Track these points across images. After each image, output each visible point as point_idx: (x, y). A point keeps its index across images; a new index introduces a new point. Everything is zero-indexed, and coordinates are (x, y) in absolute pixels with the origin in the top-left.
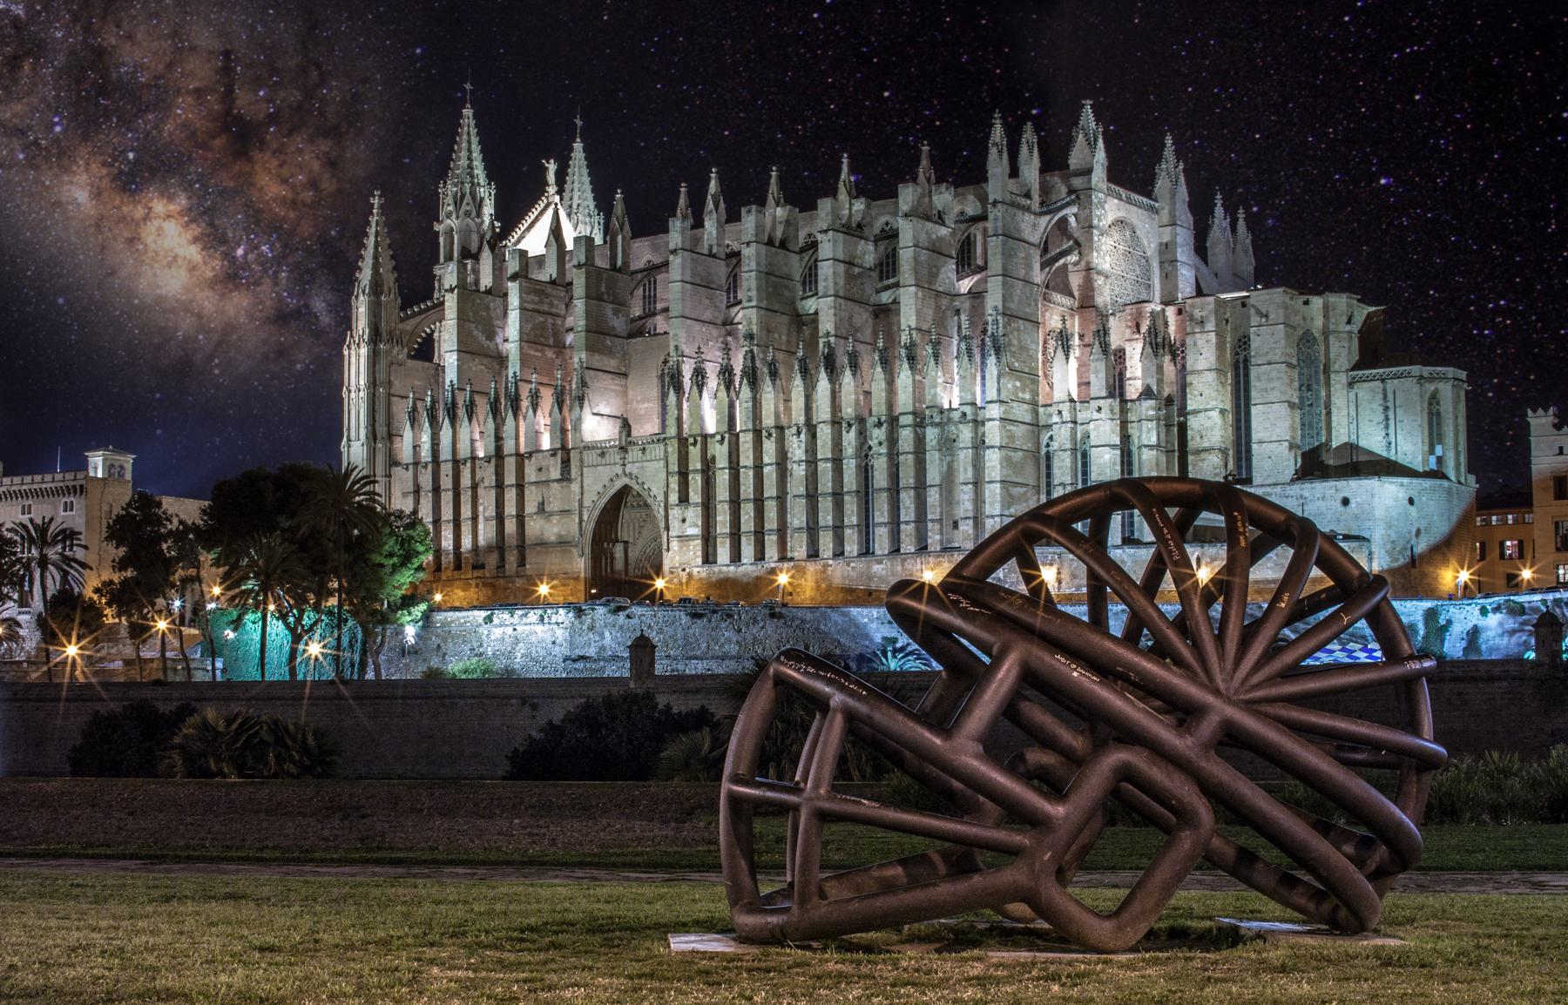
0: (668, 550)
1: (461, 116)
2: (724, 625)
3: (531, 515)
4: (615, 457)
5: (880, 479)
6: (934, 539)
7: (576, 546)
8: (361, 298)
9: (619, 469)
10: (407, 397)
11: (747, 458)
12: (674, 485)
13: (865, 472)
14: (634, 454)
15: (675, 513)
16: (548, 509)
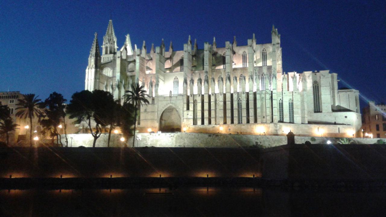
0: (183, 121)
1: (109, 21)
2: (216, 138)
3: (142, 112)
4: (169, 99)
5: (244, 105)
6: (259, 120)
7: (156, 120)
8: (92, 57)
9: (169, 102)
10: (104, 84)
11: (206, 100)
12: (185, 106)
13: (239, 105)
14: (174, 98)
15: (186, 113)
16: (147, 111)
